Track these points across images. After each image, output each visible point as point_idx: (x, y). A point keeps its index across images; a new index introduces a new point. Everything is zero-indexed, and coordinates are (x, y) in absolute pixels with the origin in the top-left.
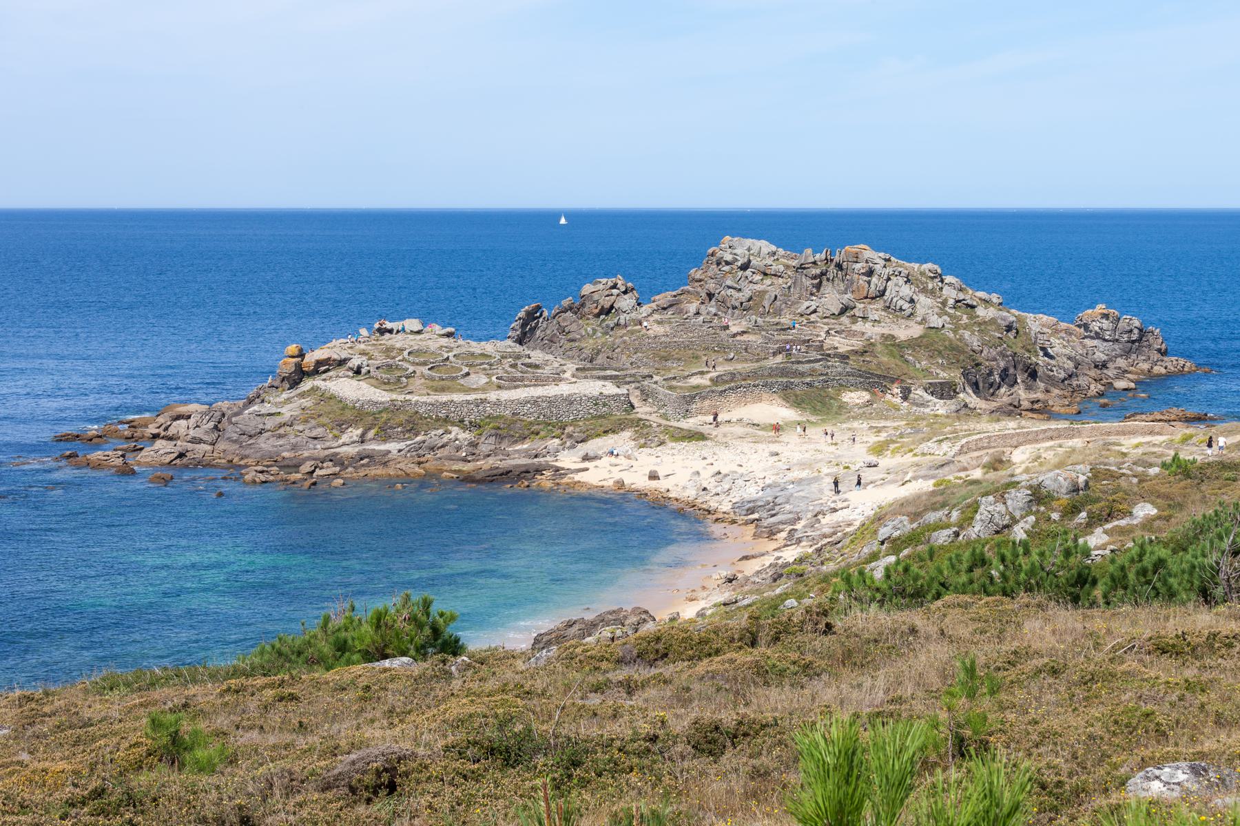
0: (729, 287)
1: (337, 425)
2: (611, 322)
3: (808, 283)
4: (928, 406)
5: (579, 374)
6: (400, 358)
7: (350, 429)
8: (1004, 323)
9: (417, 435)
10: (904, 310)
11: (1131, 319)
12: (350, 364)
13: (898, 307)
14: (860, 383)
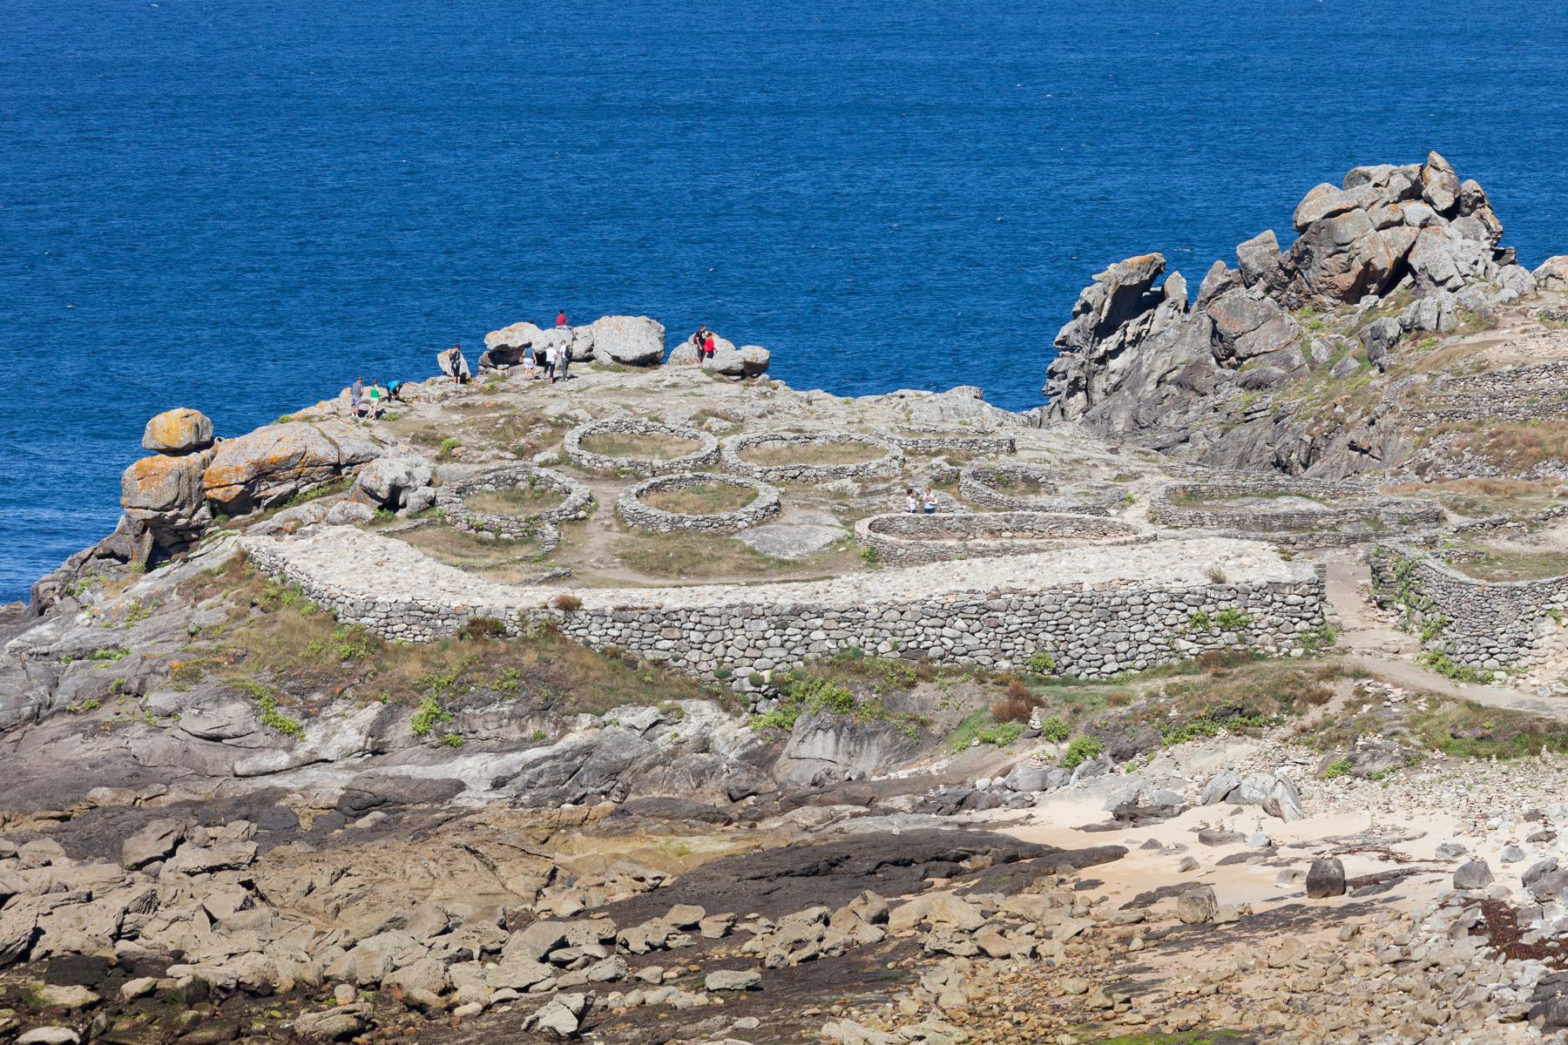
6: (551, 454)
7: (338, 707)
9: (565, 729)
12: (366, 477)
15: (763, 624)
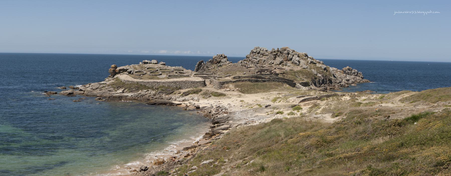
0: (254, 58)
1: (117, 87)
2: (219, 65)
3: (273, 56)
5: (195, 75)
7: (121, 89)
8: (323, 68)
10: (297, 64)
11: (355, 70)
12: (128, 71)
15: (156, 83)
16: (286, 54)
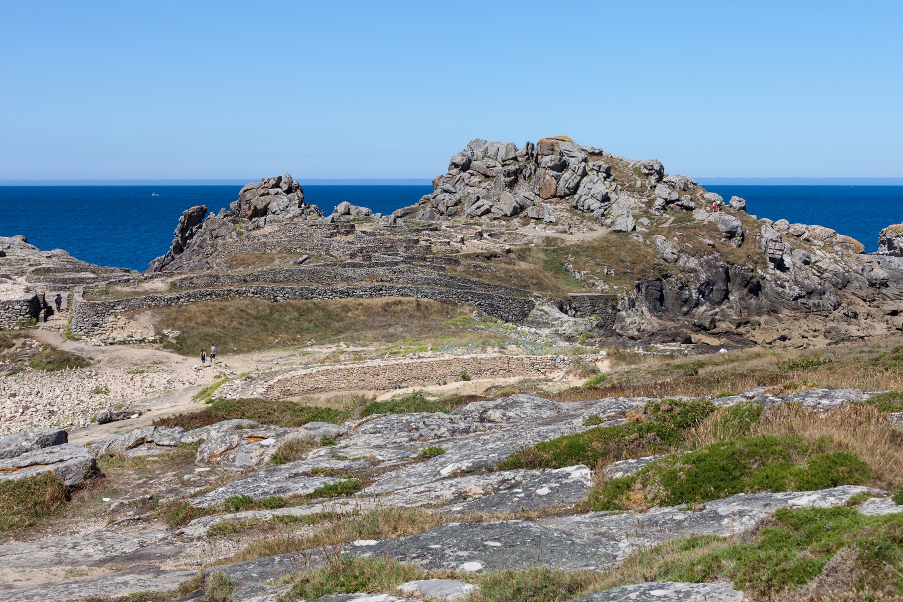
0: (446, 191)
4: (553, 325)
8: (723, 228)
10: (592, 211)
13: (586, 208)
14: (440, 293)
16: (552, 168)
